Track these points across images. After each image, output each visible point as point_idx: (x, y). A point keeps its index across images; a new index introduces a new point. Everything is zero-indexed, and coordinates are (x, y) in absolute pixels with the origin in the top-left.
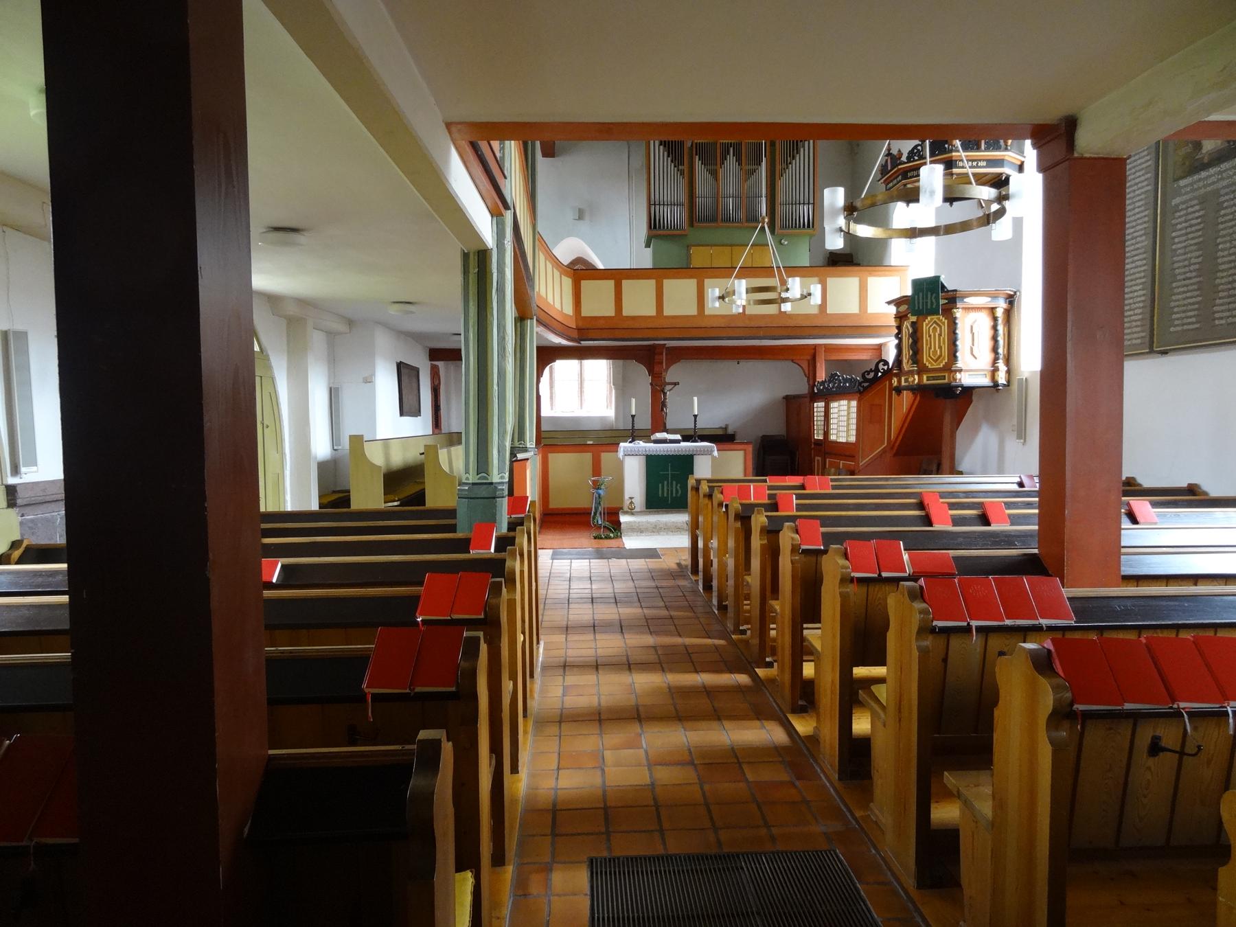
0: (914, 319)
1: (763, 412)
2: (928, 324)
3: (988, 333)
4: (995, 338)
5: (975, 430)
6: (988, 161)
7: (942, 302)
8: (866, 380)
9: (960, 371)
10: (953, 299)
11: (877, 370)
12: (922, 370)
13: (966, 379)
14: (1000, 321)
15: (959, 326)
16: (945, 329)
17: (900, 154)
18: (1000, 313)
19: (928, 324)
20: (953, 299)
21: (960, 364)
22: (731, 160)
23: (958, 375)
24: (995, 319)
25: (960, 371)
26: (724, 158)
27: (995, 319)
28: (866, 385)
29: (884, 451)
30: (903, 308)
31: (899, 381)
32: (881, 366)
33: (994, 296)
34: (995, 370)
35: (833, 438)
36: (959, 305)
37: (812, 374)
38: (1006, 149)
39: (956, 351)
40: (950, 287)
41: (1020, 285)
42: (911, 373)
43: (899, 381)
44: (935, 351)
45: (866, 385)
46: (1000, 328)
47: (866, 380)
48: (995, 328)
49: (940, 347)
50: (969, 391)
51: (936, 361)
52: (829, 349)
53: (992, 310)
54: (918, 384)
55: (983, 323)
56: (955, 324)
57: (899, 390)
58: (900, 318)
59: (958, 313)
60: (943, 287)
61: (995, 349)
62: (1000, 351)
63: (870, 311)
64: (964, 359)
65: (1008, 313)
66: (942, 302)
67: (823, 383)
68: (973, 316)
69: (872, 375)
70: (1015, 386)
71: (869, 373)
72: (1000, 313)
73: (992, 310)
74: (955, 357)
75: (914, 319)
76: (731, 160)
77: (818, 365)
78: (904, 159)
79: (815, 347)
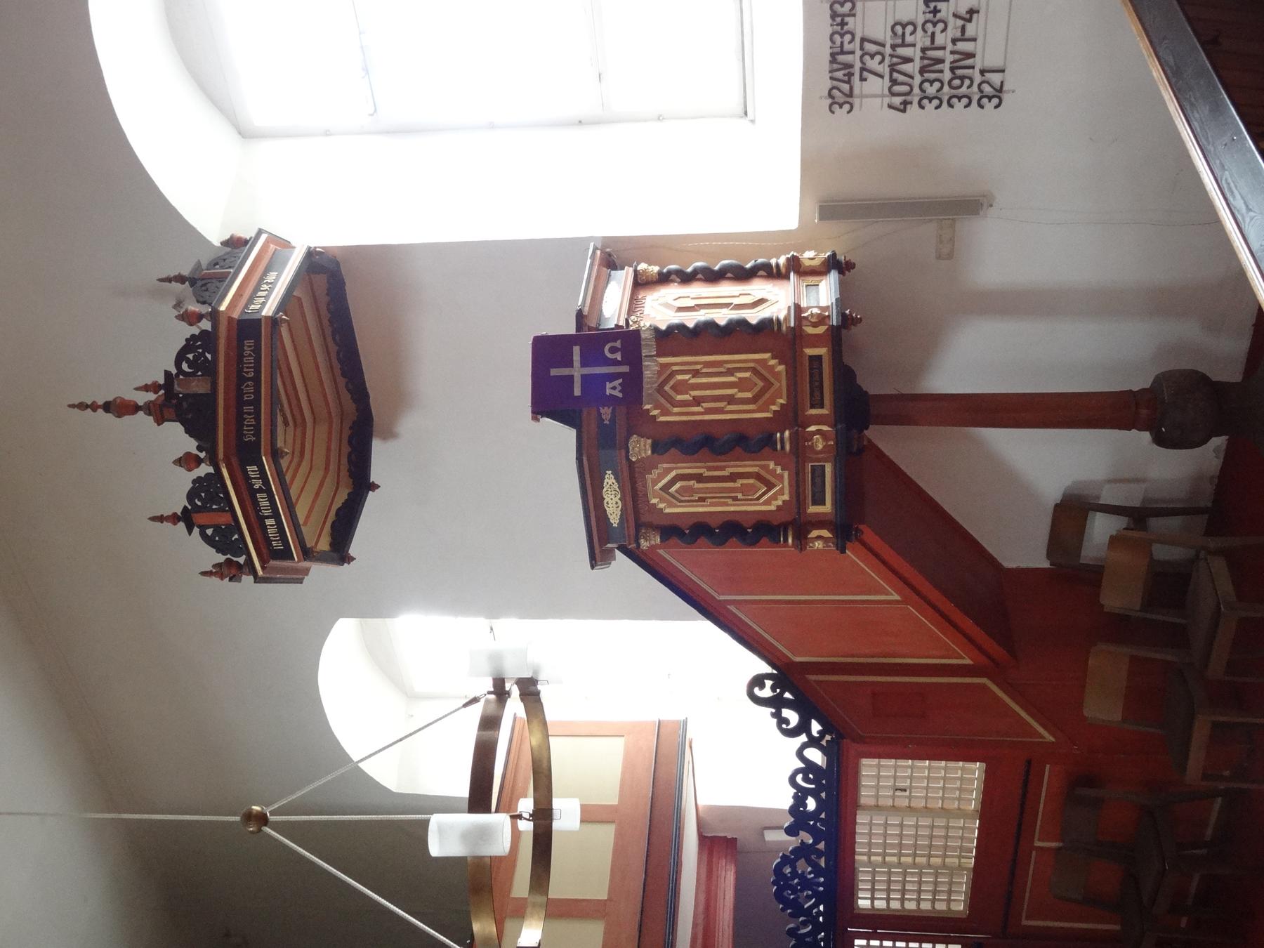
0: (640, 448)
3: (699, 291)
8: (803, 727)
9: (798, 309)
12: (792, 417)
17: (188, 461)
24: (664, 279)
25: (798, 309)
28: (816, 727)
32: (767, 693)
35: (959, 905)
41: (580, 243)
45: (816, 727)
47: (803, 727)
49: (730, 372)
51: (768, 385)
54: (834, 426)
63: (612, 799)
69: (786, 713)
71: (782, 721)
73: (641, 283)
75: (640, 448)
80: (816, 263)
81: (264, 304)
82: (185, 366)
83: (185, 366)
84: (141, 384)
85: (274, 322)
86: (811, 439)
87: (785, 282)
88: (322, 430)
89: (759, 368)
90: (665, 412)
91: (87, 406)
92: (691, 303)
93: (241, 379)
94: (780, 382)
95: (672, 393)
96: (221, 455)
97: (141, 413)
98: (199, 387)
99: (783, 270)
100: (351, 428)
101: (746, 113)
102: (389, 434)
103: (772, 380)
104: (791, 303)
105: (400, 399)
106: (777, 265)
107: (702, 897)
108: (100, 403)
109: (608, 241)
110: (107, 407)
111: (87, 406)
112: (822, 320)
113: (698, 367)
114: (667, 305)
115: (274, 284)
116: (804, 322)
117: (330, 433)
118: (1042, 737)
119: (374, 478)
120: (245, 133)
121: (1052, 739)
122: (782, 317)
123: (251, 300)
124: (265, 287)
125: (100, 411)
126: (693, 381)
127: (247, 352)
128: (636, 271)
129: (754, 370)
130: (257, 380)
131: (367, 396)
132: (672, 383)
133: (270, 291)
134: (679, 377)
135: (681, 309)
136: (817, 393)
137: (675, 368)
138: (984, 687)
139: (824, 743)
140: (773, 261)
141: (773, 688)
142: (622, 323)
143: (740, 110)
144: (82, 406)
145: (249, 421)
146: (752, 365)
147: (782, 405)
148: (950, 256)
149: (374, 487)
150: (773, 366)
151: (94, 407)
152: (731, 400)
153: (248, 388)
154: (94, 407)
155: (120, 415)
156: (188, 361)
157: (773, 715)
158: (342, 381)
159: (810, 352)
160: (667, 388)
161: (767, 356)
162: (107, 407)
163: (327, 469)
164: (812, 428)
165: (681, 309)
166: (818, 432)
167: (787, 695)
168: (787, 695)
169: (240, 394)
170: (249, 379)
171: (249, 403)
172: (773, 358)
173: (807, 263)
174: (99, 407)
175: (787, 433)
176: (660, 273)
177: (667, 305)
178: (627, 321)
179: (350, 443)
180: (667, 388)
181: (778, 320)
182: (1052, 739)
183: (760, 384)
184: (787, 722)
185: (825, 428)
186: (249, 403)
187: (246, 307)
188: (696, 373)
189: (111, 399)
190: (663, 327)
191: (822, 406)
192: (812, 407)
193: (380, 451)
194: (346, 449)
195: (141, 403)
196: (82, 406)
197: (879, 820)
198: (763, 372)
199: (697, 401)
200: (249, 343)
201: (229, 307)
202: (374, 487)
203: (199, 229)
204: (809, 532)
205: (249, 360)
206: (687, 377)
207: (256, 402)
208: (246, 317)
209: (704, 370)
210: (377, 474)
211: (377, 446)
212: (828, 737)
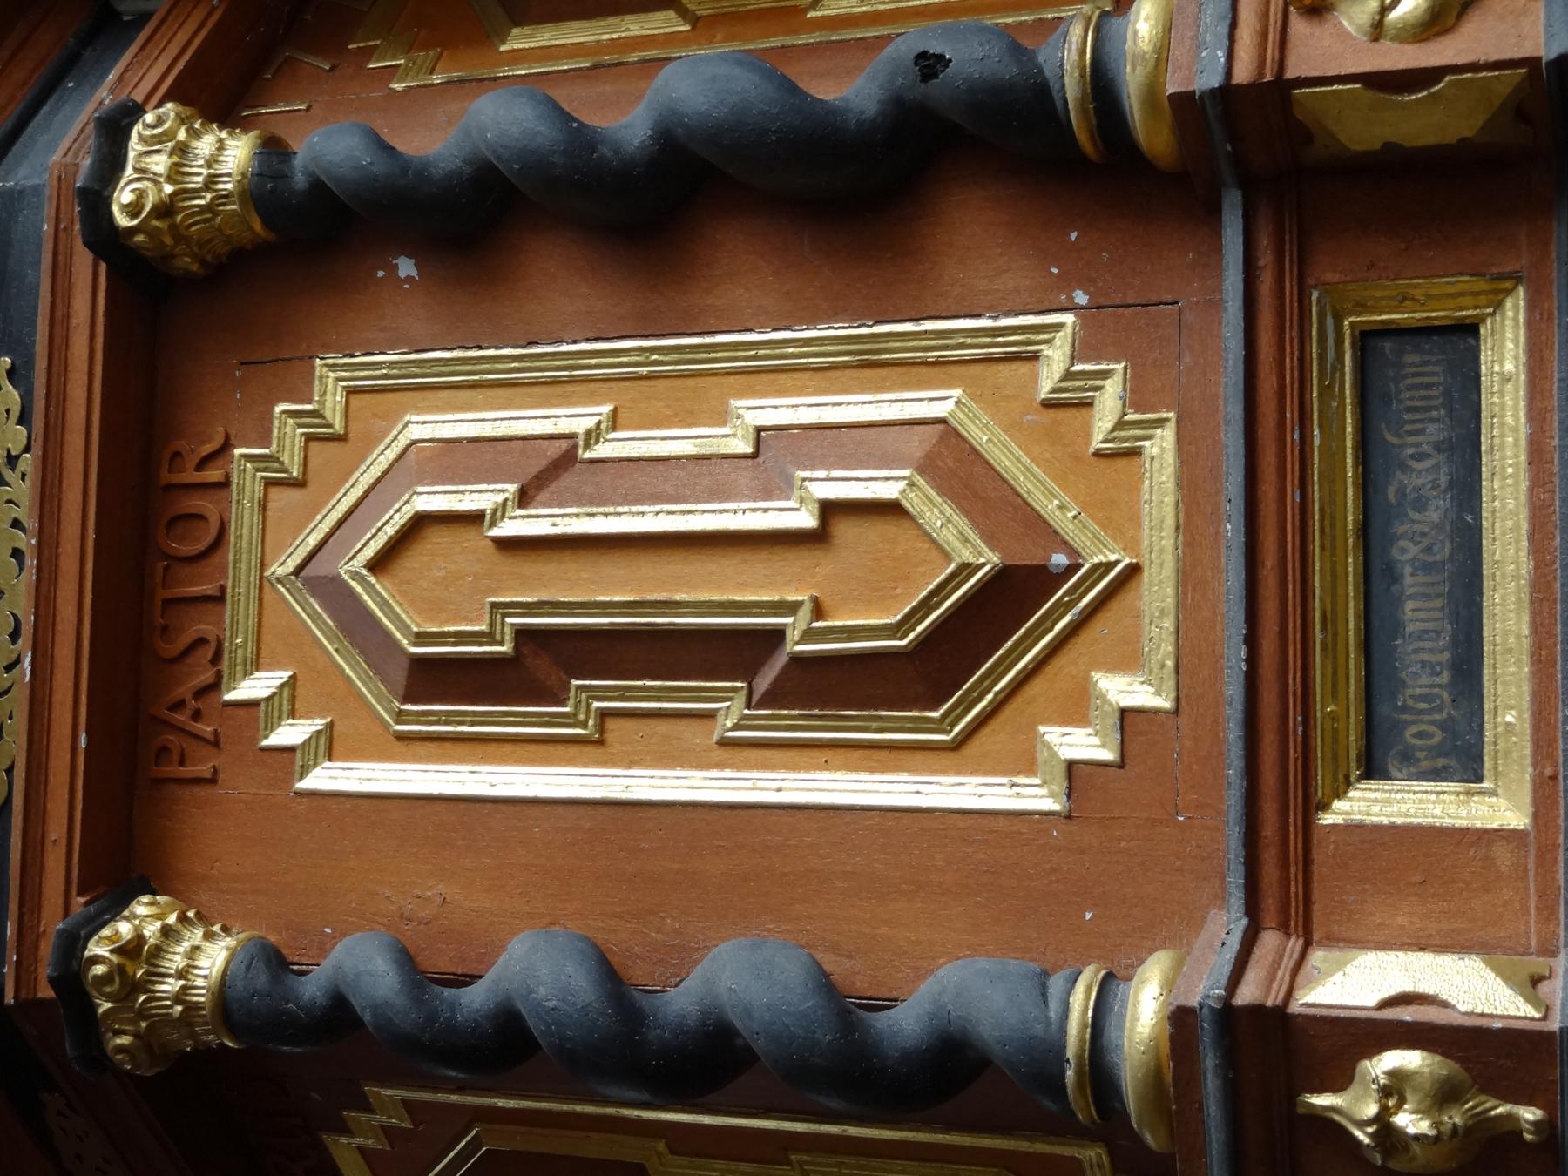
25: (1265, 1055)
80: (1418, 124)
99: (1151, 134)
106: (1102, 82)
135: (434, 678)
165: (434, 678)
173: (1365, 129)
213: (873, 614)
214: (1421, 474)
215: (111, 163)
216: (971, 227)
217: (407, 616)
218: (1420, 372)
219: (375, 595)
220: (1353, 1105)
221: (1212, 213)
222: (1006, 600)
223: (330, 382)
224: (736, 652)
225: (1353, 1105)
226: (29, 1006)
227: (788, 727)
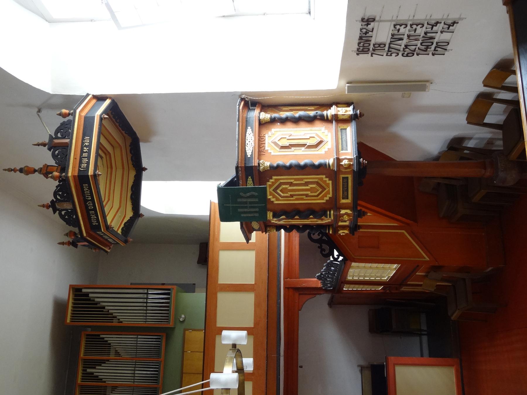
1: (345, 328)
2: (277, 198)
4: (296, 121)
5: (395, 138)
6: (84, 135)
7: (250, 184)
9: (338, 160)
10: (247, 171)
11: (319, 241)
12: (334, 204)
13: (349, 153)
14: (275, 115)
15: (281, 162)
16: (283, 179)
18: (265, 116)
19: (277, 198)
20: (247, 171)
21: (331, 161)
22: (99, 371)
23: (345, 162)
24: (273, 121)
25: (338, 160)
26: (97, 379)
27: (273, 121)
28: (336, 253)
29: (412, 234)
30: (255, 225)
31: (344, 227)
32: (316, 236)
33: (245, 124)
34: (336, 119)
36: (255, 163)
37: (313, 291)
38: (74, 115)
39: (313, 166)
40: (233, 174)
42: (338, 217)
43: (344, 227)
44: (311, 190)
46: (284, 114)
48: (284, 121)
49: (307, 184)
50: (362, 148)
51: (324, 189)
52: (289, 274)
53: (262, 124)
55: (276, 135)
56: (278, 166)
57: (354, 228)
58: (266, 227)
59: (266, 163)
60: (231, 183)
61: (310, 120)
62: (312, 113)
64: (325, 155)
65: (265, 107)
66: (250, 184)
67: (324, 284)
68: (269, 146)
69: (325, 246)
70: (355, 96)
71: (322, 250)
72: (265, 116)
74: (320, 166)
76: (99, 371)
77: (304, 285)
78: (76, 230)
79: (285, 288)
80: (344, 117)
81: (88, 163)
82: (59, 197)
83: (59, 197)
84: (41, 204)
85: (95, 176)
86: (343, 217)
87: (329, 125)
88: (118, 152)
89: (320, 182)
90: (278, 200)
91: (12, 170)
92: (286, 143)
93: (86, 201)
94: (329, 188)
95: (280, 193)
96: (85, 235)
97: (37, 173)
98: (68, 206)
99: (329, 118)
100: (130, 146)
101: (310, 13)
102: (147, 141)
103: (325, 187)
104: (335, 157)
105: (150, 133)
107: (287, 250)
108: (18, 168)
109: (242, 93)
110: (21, 170)
111: (12, 170)
112: (350, 166)
113: (292, 181)
114: (275, 144)
115: (90, 146)
116: (341, 167)
117: (121, 151)
118: (425, 258)
119: (144, 165)
120: (50, 21)
121: (427, 259)
122: (331, 163)
123: (81, 162)
124: (86, 149)
125: (18, 172)
126: (290, 188)
127: (86, 189)
128: (259, 120)
129: (317, 183)
130: (93, 200)
131: (135, 133)
132: (280, 188)
133: (89, 152)
134: (284, 186)
135: (283, 147)
136: (346, 193)
137: (282, 181)
138: (403, 233)
139: (339, 260)
140: (325, 113)
141: (319, 235)
142: (256, 164)
143: (307, 11)
144: (10, 170)
145: (93, 217)
146: (316, 180)
147: (330, 198)
148: (409, 97)
149: (145, 169)
150: (326, 181)
151: (15, 170)
152: (307, 195)
153: (90, 204)
154: (15, 170)
155: (27, 174)
156: (59, 195)
157: (319, 247)
158: (123, 132)
159: (342, 176)
160: (278, 191)
161: (324, 176)
162: (21, 170)
163: (123, 168)
164: (343, 212)
166: (346, 214)
167: (324, 238)
168: (324, 238)
169: (87, 207)
170: (89, 200)
171: (91, 210)
172: (326, 177)
173: (341, 117)
174: (17, 170)
175: (332, 212)
176: (271, 118)
177: (275, 144)
178: (259, 164)
179: (131, 152)
180: (278, 191)
181: (329, 164)
182: (427, 259)
183: (320, 190)
184: (324, 250)
185: (349, 211)
186: (91, 210)
187: (80, 167)
188: (291, 184)
189: (23, 167)
190: (275, 165)
191: (348, 198)
192: (343, 199)
193: (144, 149)
194: (130, 156)
195: (37, 169)
196: (10, 170)
197: (357, 271)
198: (321, 183)
199: (292, 196)
200: (85, 186)
201: (72, 173)
202: (145, 169)
203: (42, 89)
204: (339, 231)
205: (87, 192)
206: (287, 186)
207: (95, 209)
208: (82, 174)
209: (295, 182)
210: (144, 165)
211: (143, 147)
212: (341, 258)
213: (313, 142)
214: (344, 136)
215: (260, 115)
216: (318, 123)
217: (281, 143)
218: (344, 131)
219: (278, 142)
220: (343, 163)
221: (332, 122)
222: (321, 142)
223: (273, 130)
224: (303, 145)
225: (343, 163)
226: (255, 166)
227: (307, 150)
